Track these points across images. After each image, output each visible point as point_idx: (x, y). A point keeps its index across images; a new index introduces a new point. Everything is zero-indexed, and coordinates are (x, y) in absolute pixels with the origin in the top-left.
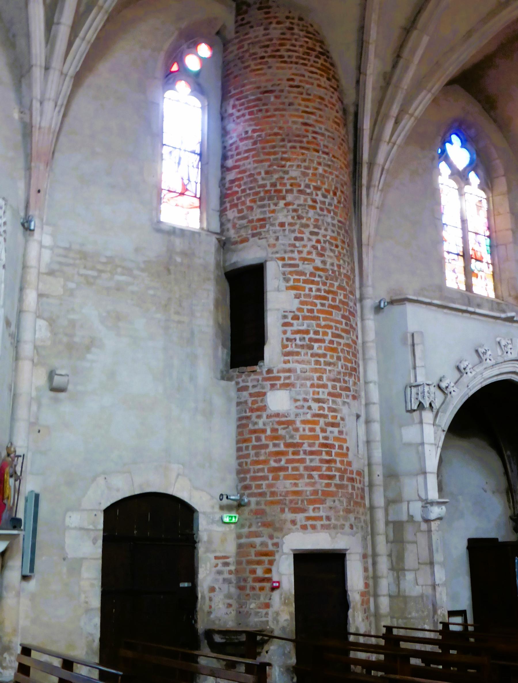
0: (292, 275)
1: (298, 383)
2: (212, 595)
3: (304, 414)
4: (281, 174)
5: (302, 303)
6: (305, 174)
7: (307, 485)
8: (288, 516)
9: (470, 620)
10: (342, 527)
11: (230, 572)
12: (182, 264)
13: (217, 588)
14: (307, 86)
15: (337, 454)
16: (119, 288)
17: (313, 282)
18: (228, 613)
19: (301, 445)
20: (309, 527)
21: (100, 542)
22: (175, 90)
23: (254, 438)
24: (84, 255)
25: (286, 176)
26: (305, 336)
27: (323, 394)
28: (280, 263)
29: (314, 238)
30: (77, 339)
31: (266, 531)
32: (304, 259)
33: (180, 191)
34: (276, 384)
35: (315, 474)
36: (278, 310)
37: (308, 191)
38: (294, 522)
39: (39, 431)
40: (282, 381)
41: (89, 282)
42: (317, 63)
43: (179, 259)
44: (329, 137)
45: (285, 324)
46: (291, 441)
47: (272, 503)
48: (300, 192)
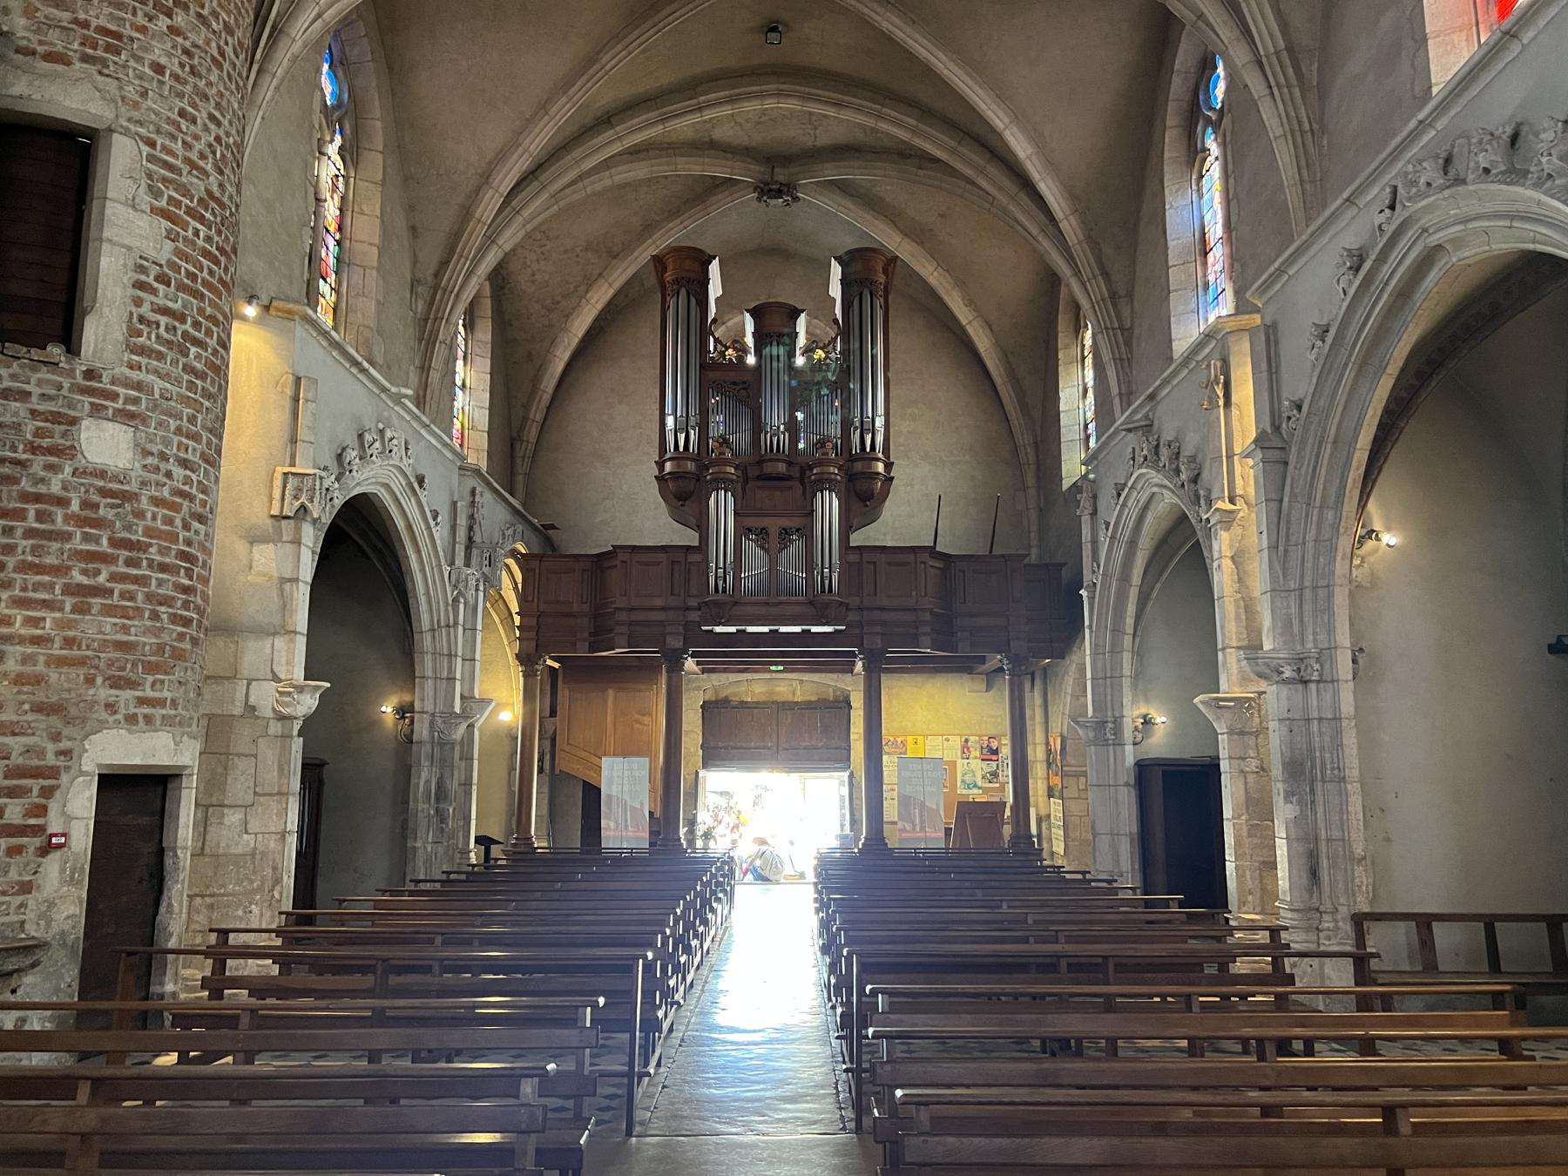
0: (167, 188)
1: (155, 417)
3: (157, 484)
5: (178, 253)
7: (147, 631)
8: (104, 693)
19: (143, 548)
20: (141, 719)
23: (32, 514)
28: (146, 149)
31: (40, 721)
36: (129, 248)
38: (111, 707)
40: (119, 405)
46: (125, 535)
47: (62, 662)
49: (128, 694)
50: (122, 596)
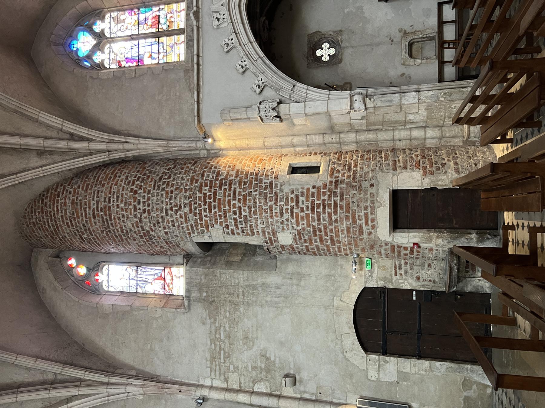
2: (421, 279)
3: (292, 224)
4: (133, 232)
5: (216, 223)
6: (128, 218)
7: (342, 224)
8: (365, 236)
10: (372, 195)
11: (406, 263)
12: (207, 292)
13: (417, 275)
14: (68, 214)
17: (201, 215)
18: (435, 267)
20: (373, 224)
21: (387, 358)
24: (213, 359)
25: (133, 229)
26: (238, 221)
27: (276, 209)
28: (192, 235)
29: (170, 212)
30: (263, 366)
32: (186, 221)
34: (274, 240)
35: (334, 217)
37: (139, 216)
38: (370, 234)
39: (320, 393)
42: (50, 205)
43: (205, 294)
44: (98, 197)
45: (233, 233)
48: (141, 221)
49: (365, 229)
50: (332, 232)
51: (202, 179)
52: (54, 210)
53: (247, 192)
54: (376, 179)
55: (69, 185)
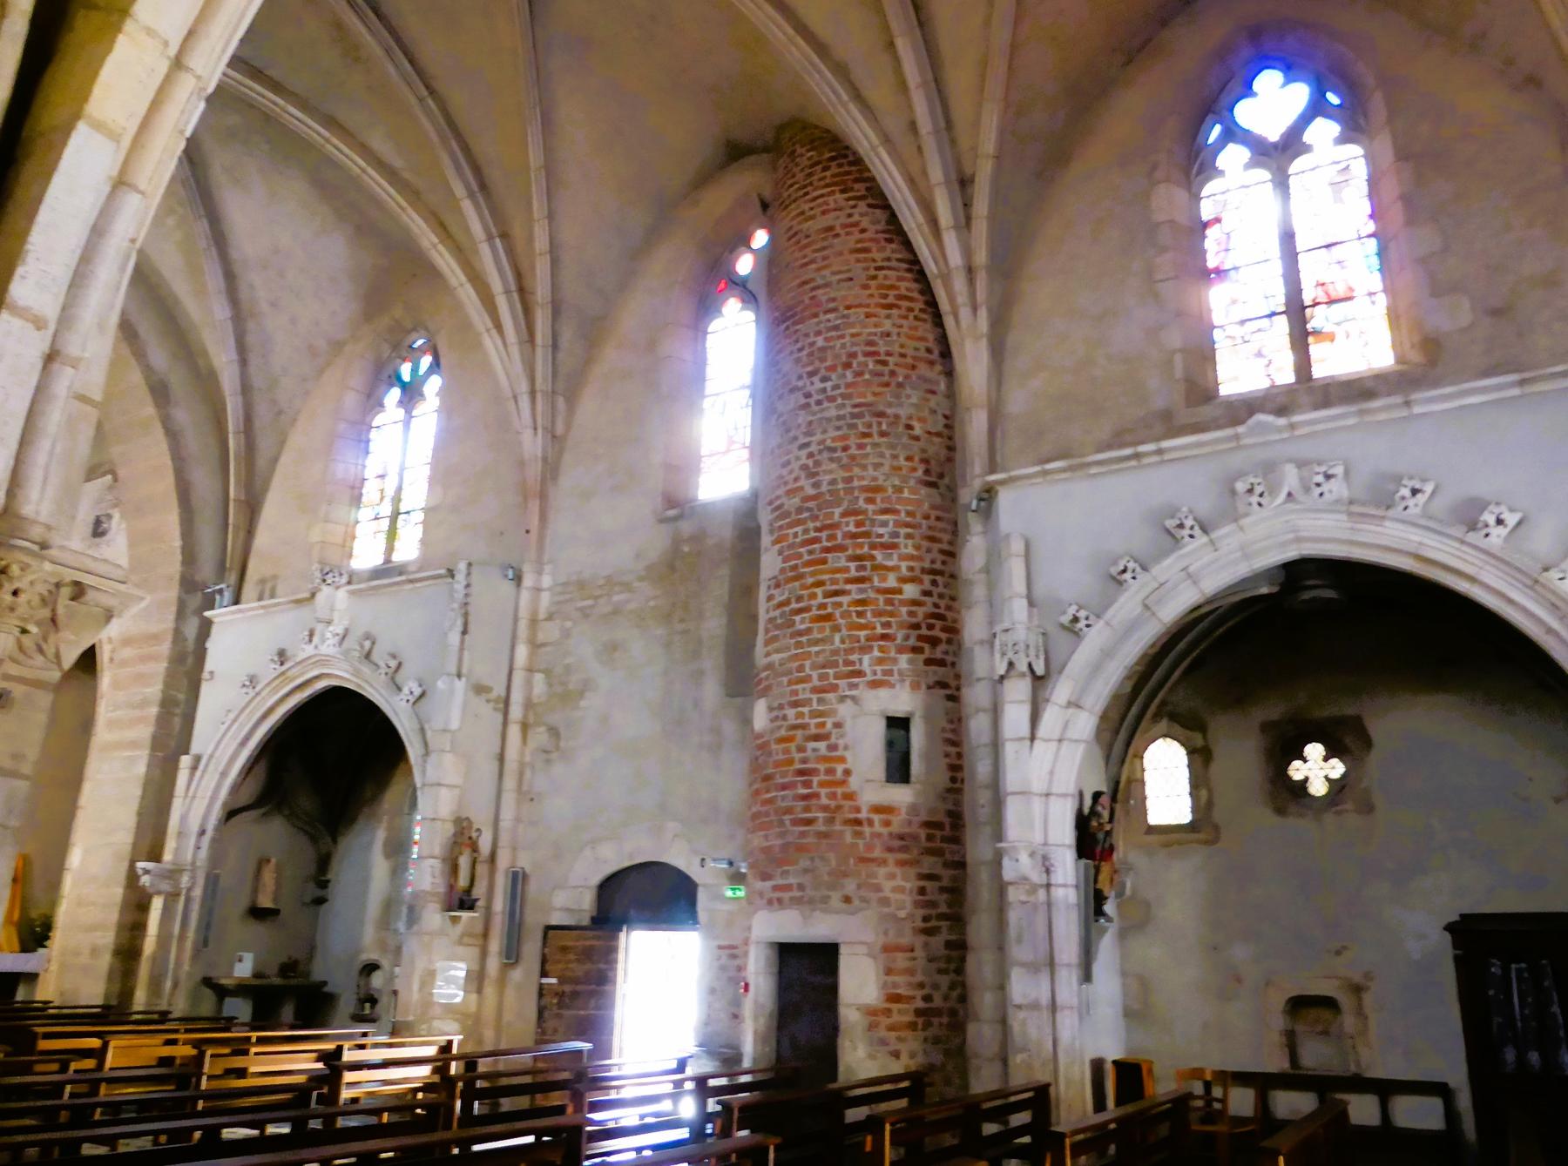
9: (1464, 1101)
15: (822, 784)
16: (616, 611)
22: (1221, 173)
24: (581, 585)
27: (803, 690)
29: (804, 453)
30: (571, 687)
33: (723, 449)
37: (800, 384)
41: (585, 613)
44: (840, 281)
51: (875, 513)
52: (815, 190)
53: (841, 621)
54: (861, 909)
55: (870, 206)
